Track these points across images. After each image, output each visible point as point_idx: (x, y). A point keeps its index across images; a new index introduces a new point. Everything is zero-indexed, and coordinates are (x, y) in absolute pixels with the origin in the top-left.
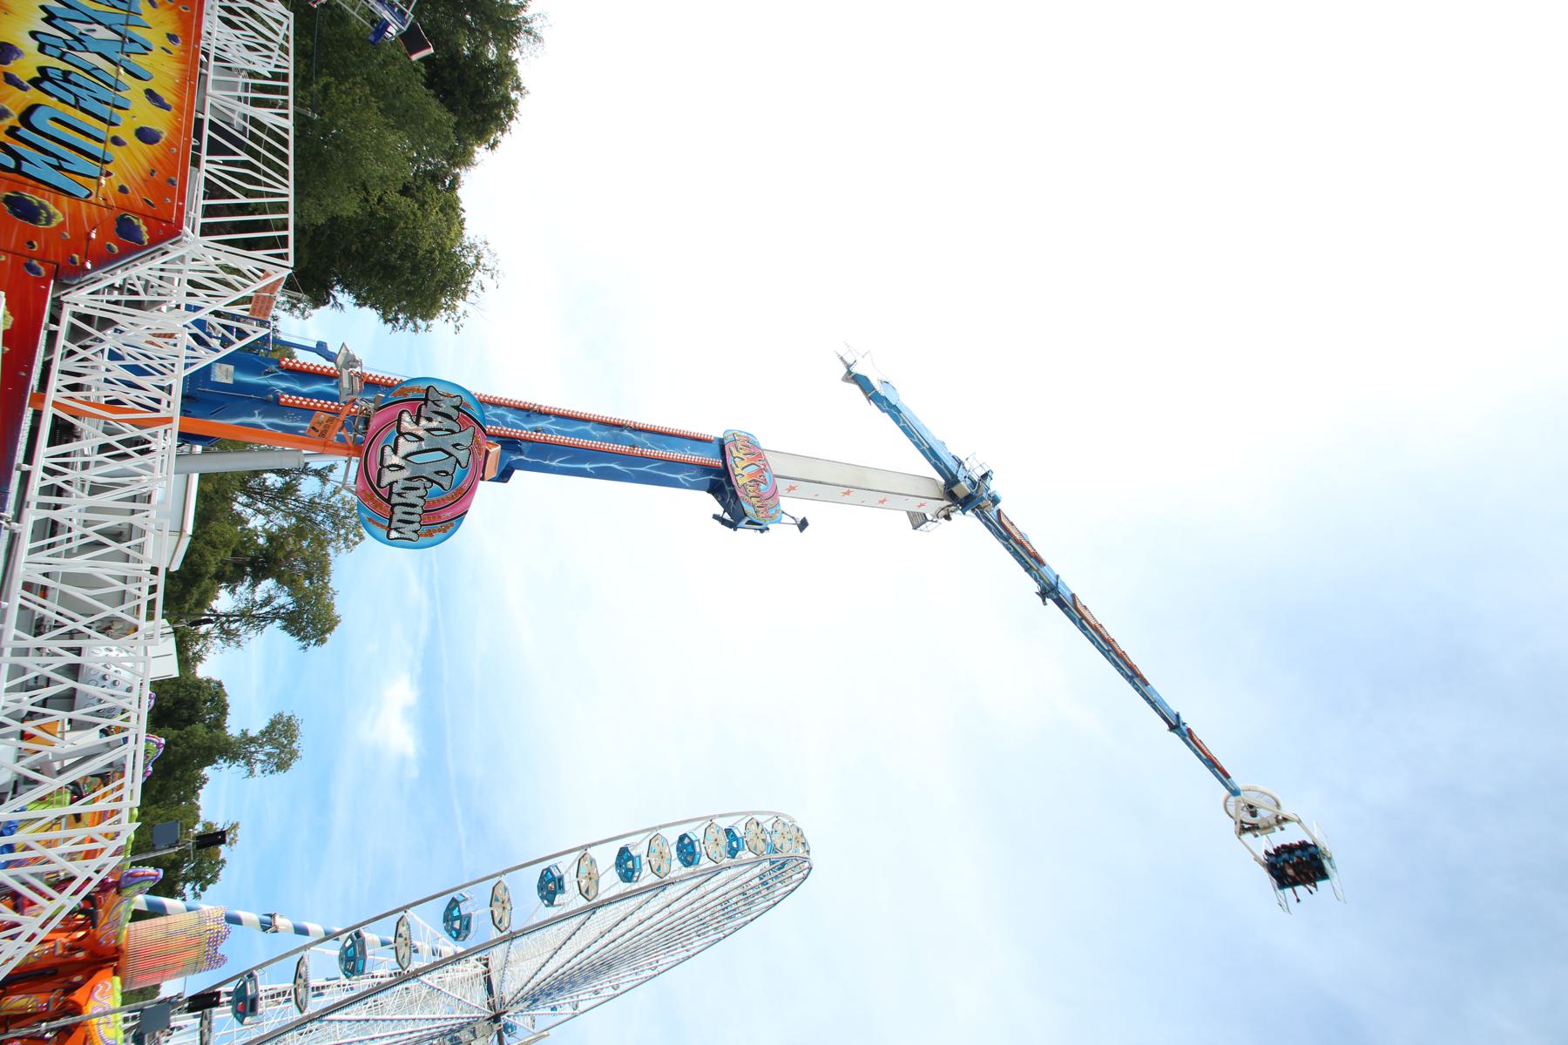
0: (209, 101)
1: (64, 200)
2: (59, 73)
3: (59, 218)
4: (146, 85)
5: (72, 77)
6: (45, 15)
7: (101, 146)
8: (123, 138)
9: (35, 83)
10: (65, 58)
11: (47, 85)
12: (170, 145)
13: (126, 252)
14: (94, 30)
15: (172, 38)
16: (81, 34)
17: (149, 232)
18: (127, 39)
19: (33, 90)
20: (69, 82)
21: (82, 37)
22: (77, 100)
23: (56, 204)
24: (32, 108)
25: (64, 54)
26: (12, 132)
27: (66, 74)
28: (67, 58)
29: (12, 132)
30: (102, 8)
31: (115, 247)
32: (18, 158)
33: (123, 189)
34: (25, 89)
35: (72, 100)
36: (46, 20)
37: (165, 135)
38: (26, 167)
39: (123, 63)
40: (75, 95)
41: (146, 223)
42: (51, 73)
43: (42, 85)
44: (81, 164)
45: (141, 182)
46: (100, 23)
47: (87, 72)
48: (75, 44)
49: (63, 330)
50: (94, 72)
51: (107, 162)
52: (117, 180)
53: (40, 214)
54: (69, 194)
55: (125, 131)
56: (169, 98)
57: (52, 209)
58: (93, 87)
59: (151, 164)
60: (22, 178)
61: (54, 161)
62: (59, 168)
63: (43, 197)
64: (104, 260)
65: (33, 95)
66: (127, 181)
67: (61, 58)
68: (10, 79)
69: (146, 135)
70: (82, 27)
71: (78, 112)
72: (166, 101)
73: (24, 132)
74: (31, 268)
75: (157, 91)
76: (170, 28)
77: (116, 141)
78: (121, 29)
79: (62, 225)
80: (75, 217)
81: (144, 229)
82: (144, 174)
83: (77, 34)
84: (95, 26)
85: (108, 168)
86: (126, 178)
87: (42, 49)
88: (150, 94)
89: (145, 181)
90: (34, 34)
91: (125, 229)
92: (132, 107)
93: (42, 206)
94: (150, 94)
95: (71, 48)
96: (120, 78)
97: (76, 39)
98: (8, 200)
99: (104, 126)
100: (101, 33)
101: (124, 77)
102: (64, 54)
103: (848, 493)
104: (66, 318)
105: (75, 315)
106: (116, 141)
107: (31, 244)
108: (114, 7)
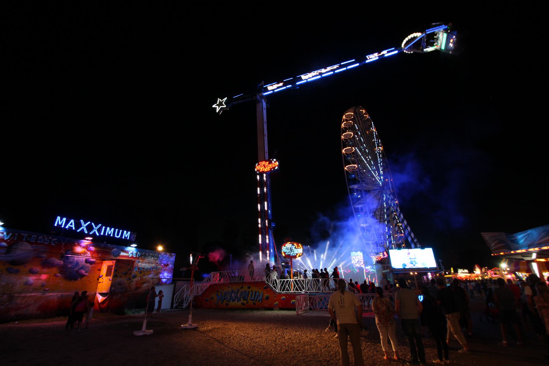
0: (238, 281)
1: (264, 295)
4: (240, 289)
5: (243, 296)
6: (234, 302)
7: (254, 293)
9: (246, 300)
11: (246, 299)
13: (269, 287)
15: (229, 287)
18: (232, 292)
19: (248, 300)
23: (265, 295)
24: (251, 300)
26: (256, 301)
27: (243, 298)
29: (256, 301)
32: (260, 300)
33: (260, 289)
34: (248, 301)
36: (235, 301)
38: (261, 298)
40: (246, 296)
44: (257, 294)
46: (231, 295)
48: (237, 297)
49: (283, 292)
50: (241, 294)
54: (263, 294)
55: (250, 290)
61: (258, 297)
62: (259, 296)
64: (271, 289)
65: (248, 300)
67: (241, 298)
68: (247, 303)
69: (249, 288)
73: (255, 300)
74: (276, 296)
77: (252, 291)
84: (232, 295)
85: (257, 291)
87: (240, 301)
90: (238, 302)
91: (266, 288)
94: (242, 288)
97: (236, 297)
98: (267, 300)
99: (250, 293)
100: (233, 295)
101: (240, 291)
103: (265, 135)
104: (281, 292)
105: (280, 291)
106: (252, 291)
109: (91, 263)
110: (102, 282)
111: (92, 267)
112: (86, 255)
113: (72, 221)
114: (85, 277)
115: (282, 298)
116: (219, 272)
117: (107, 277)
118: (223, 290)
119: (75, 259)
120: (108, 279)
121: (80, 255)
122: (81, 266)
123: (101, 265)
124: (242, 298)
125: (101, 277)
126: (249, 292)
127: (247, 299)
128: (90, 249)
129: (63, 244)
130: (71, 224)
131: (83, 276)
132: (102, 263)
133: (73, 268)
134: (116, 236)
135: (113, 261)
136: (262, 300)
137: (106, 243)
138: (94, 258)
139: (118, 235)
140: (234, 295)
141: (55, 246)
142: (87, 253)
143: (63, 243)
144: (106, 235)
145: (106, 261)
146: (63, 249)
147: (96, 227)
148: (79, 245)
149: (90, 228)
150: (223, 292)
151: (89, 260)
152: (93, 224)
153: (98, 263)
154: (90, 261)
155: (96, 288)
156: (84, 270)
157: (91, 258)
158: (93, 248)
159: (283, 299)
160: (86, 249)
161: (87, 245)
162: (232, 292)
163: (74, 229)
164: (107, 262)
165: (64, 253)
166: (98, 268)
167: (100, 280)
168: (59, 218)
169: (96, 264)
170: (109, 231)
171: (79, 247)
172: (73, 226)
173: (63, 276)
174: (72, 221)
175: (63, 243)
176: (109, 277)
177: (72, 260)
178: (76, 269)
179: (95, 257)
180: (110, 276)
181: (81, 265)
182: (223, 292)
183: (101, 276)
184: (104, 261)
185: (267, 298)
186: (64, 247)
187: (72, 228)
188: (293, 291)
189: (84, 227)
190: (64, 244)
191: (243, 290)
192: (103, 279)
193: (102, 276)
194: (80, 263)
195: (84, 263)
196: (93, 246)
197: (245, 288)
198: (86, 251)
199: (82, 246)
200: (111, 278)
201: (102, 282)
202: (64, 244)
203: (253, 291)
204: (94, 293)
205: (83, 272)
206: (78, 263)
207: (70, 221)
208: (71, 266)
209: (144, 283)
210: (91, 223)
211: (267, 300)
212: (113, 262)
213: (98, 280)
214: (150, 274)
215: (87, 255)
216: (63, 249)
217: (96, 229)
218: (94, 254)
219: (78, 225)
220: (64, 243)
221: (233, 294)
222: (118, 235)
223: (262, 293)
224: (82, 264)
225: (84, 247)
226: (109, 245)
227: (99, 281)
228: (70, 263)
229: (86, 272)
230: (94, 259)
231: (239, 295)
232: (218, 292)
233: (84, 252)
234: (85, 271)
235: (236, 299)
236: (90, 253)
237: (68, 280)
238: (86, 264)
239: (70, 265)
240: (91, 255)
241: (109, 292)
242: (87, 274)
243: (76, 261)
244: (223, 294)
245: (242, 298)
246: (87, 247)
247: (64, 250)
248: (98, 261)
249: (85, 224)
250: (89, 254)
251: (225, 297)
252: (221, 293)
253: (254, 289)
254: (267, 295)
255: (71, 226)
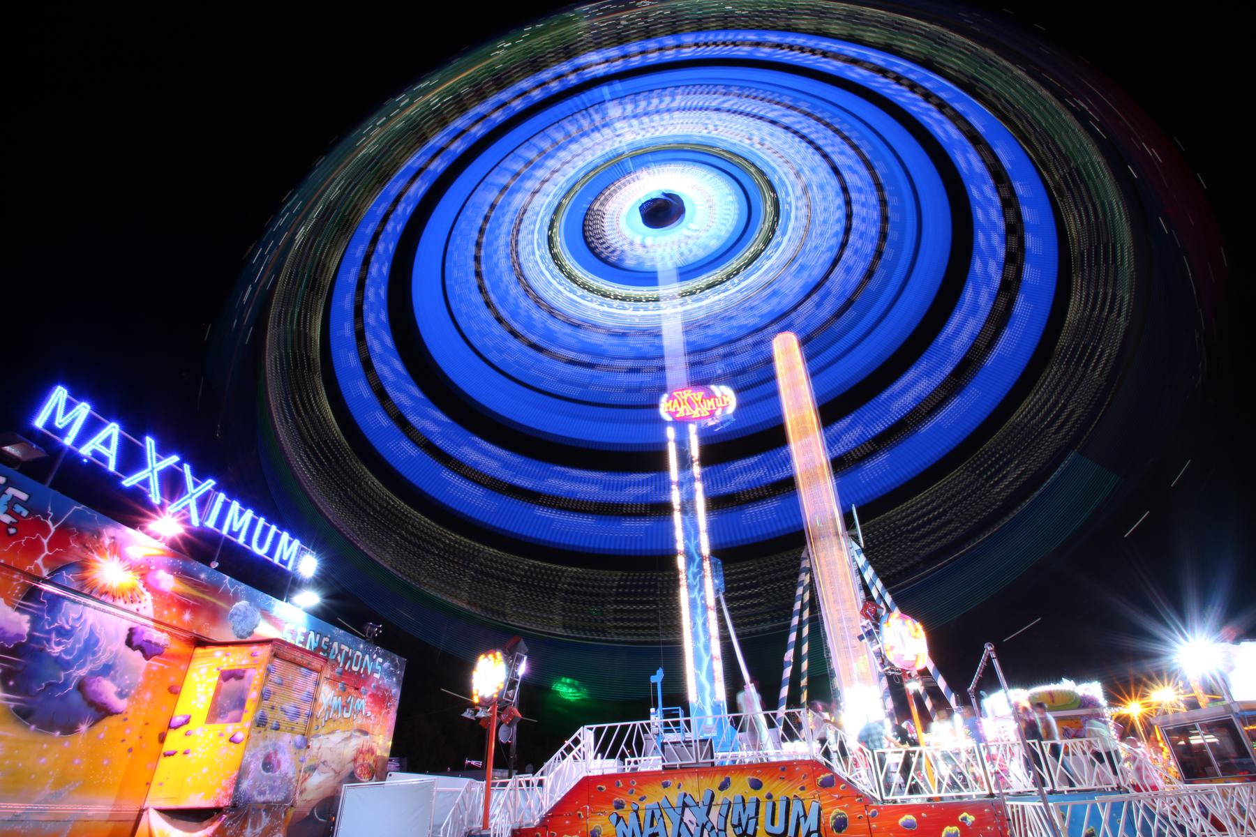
0: (701, 760)
2: (737, 829)
3: (838, 810)
4: (717, 793)
5: (736, 823)
8: (765, 794)
10: (723, 828)
12: (755, 773)
14: (690, 821)
15: (666, 785)
16: (697, 826)
17: (824, 773)
18: (685, 805)
20: (740, 825)
21: (700, 825)
22: (751, 818)
23: (830, 813)
25: (719, 830)
27: (734, 826)
28: (723, 828)
30: (667, 820)
31: (842, 786)
33: (802, 789)
35: (752, 822)
37: (751, 777)
38: (814, 828)
39: (707, 802)
40: (748, 819)
41: (819, 776)
42: (739, 831)
43: (752, 834)
44: (796, 808)
45: (791, 784)
46: (682, 820)
47: (726, 818)
48: (709, 826)
49: (898, 798)
51: (788, 798)
52: (799, 793)
53: (840, 818)
54: (820, 809)
55: (761, 794)
56: (719, 780)
57: (834, 813)
58: (736, 814)
59: (777, 779)
60: (822, 829)
61: (802, 820)
62: (805, 816)
63: (828, 819)
66: (796, 788)
67: (725, 830)
69: (756, 785)
70: (692, 828)
71: (760, 816)
72: (723, 780)
74: (874, 814)
75: (718, 785)
76: (660, 788)
77: (770, 796)
78: (679, 811)
79: (840, 808)
80: (834, 805)
81: (822, 776)
82: (786, 782)
83: (700, 828)
84: (686, 819)
85: (791, 797)
86: (795, 788)
88: (723, 787)
89: (790, 781)
91: (827, 784)
92: (739, 794)
93: (834, 818)
94: (723, 787)
95: (713, 828)
96: (720, 802)
97: (704, 826)
98: (839, 830)
100: (688, 816)
102: (719, 830)
104: (890, 797)
106: (770, 796)
107: (859, 818)
108: (662, 815)
109: (149, 650)
110: (186, 753)
111: (148, 672)
112: (133, 607)
113: (113, 430)
114: (110, 723)
115: (901, 821)
116: (591, 729)
117: (218, 727)
118: (642, 799)
119: (85, 621)
120: (221, 735)
121: (110, 600)
122: (103, 658)
123: (182, 667)
124: (729, 828)
125: (175, 728)
126: (758, 802)
127: (755, 831)
128: (157, 582)
129: (48, 530)
130: (107, 443)
131: (103, 711)
132: (189, 659)
133: (67, 665)
134: (255, 548)
135: (254, 648)
136: (818, 831)
137: (216, 569)
138: (162, 627)
139: (261, 543)
140: (694, 820)
141: (12, 531)
142: (143, 598)
143: (50, 523)
144: (225, 531)
145: (210, 650)
146: (47, 552)
147: (196, 485)
148: (117, 549)
149: (173, 484)
150: (642, 805)
151: (143, 633)
152: (187, 469)
153: (175, 657)
154: (145, 637)
155: (148, 784)
156: (113, 679)
157: (151, 623)
158: (167, 581)
159: (907, 825)
160: (142, 575)
161: (148, 559)
162: (685, 805)
163: (112, 467)
164: (218, 652)
165: (45, 573)
166: (172, 680)
167: (174, 740)
168: (60, 394)
169: (167, 656)
170: (236, 517)
171: (116, 559)
172: (111, 454)
173: (12, 705)
174: (113, 430)
175: (50, 523)
176: (229, 728)
177: (75, 620)
178: (83, 672)
179: (168, 621)
180: (238, 720)
181: (107, 654)
182: (642, 805)
183: (178, 719)
184: (199, 651)
185: (841, 824)
186: (51, 545)
187: (104, 459)
188: (939, 791)
189: (152, 471)
190: (53, 529)
191: (732, 794)
192: (188, 734)
193: (187, 721)
194: (103, 643)
195: (120, 645)
196: (171, 570)
197: (740, 787)
198: (140, 585)
199: (130, 560)
200: (242, 729)
201: (186, 753)
202: (53, 529)
203: (774, 798)
204: (133, 808)
205: (108, 689)
206: (97, 641)
207: (102, 426)
208: (60, 648)
209: (313, 769)
210: (180, 464)
211: (839, 830)
212: (253, 655)
213: (162, 739)
214: (332, 732)
215: (141, 606)
216: (47, 552)
217: (193, 494)
218: (168, 606)
219: (131, 458)
220: (54, 521)
221: (687, 810)
222: (261, 543)
223: (815, 806)
224: (109, 648)
225: (133, 567)
226: (228, 578)
227: (168, 746)
228: (63, 633)
229: (121, 695)
230: (163, 631)
231: (714, 816)
232: (620, 806)
233: (133, 590)
234: (119, 687)
235: (706, 832)
236: (154, 601)
237: (33, 727)
238: (129, 650)
239: (59, 644)
240: (155, 611)
241: (225, 802)
242: (121, 704)
243: (87, 630)
244: (641, 814)
245: (729, 828)
246: (144, 570)
247: (47, 555)
248: (176, 647)
249: (158, 460)
250: (147, 604)
251: (652, 825)
252: (636, 812)
253: (780, 790)
254: (838, 810)
255: (103, 450)
